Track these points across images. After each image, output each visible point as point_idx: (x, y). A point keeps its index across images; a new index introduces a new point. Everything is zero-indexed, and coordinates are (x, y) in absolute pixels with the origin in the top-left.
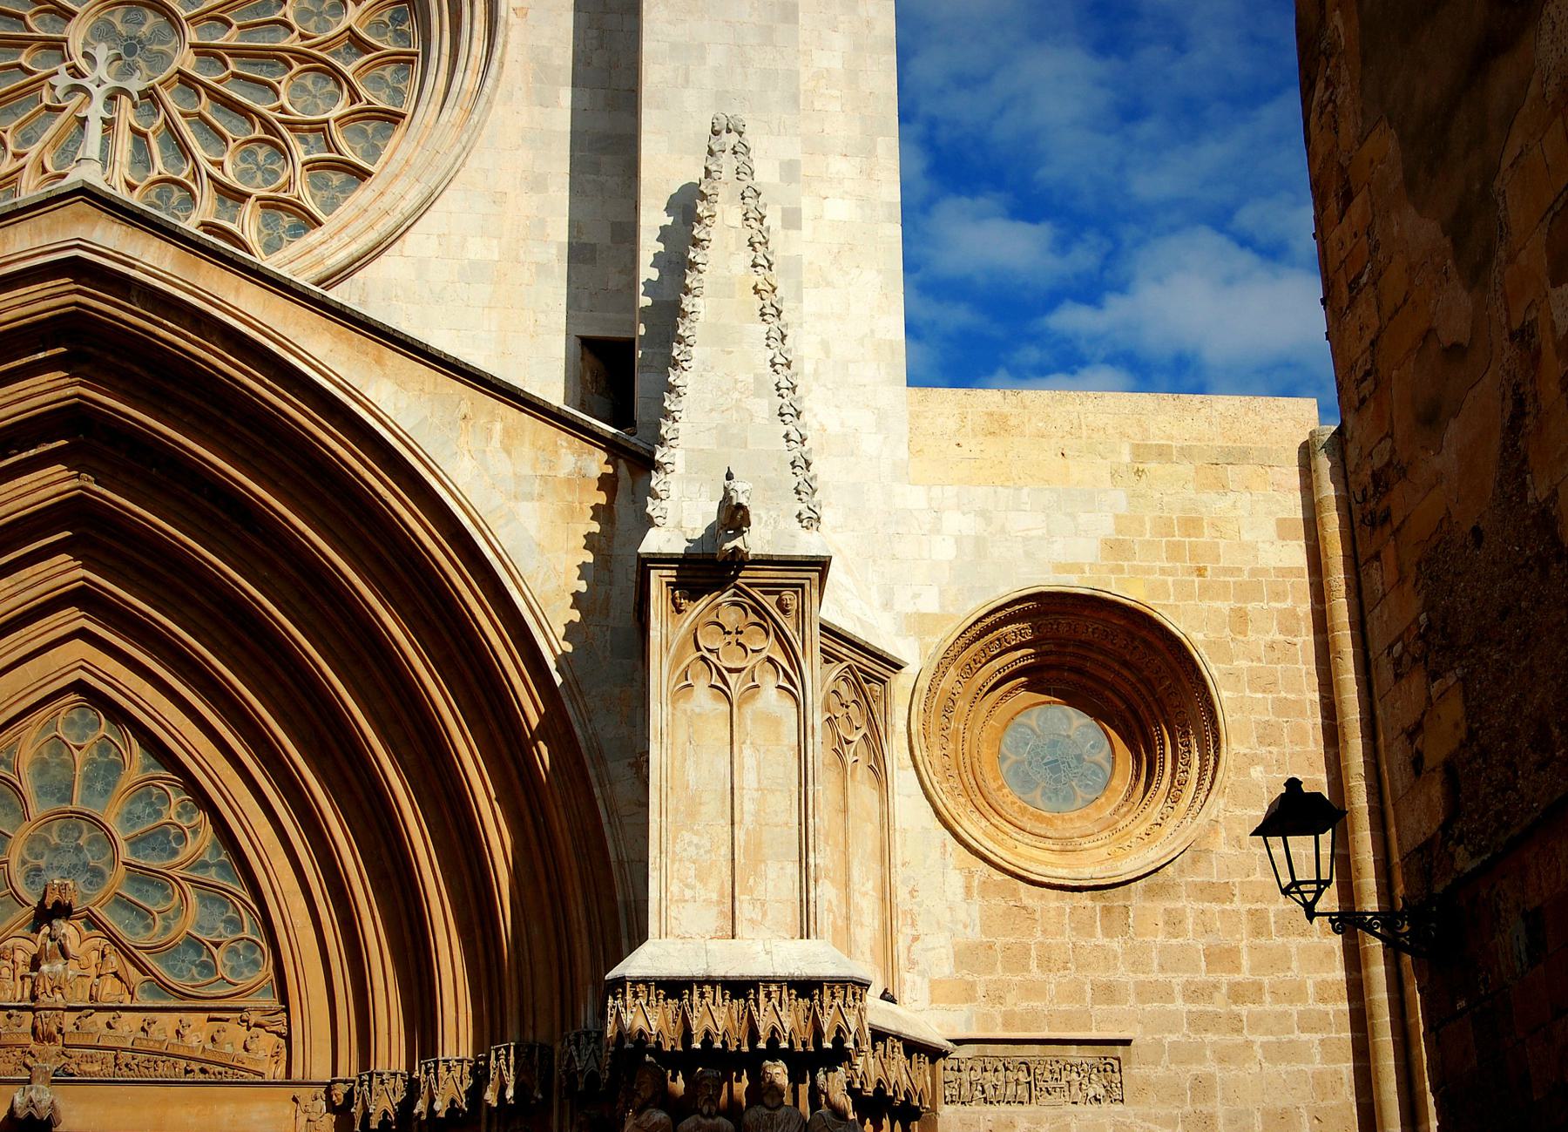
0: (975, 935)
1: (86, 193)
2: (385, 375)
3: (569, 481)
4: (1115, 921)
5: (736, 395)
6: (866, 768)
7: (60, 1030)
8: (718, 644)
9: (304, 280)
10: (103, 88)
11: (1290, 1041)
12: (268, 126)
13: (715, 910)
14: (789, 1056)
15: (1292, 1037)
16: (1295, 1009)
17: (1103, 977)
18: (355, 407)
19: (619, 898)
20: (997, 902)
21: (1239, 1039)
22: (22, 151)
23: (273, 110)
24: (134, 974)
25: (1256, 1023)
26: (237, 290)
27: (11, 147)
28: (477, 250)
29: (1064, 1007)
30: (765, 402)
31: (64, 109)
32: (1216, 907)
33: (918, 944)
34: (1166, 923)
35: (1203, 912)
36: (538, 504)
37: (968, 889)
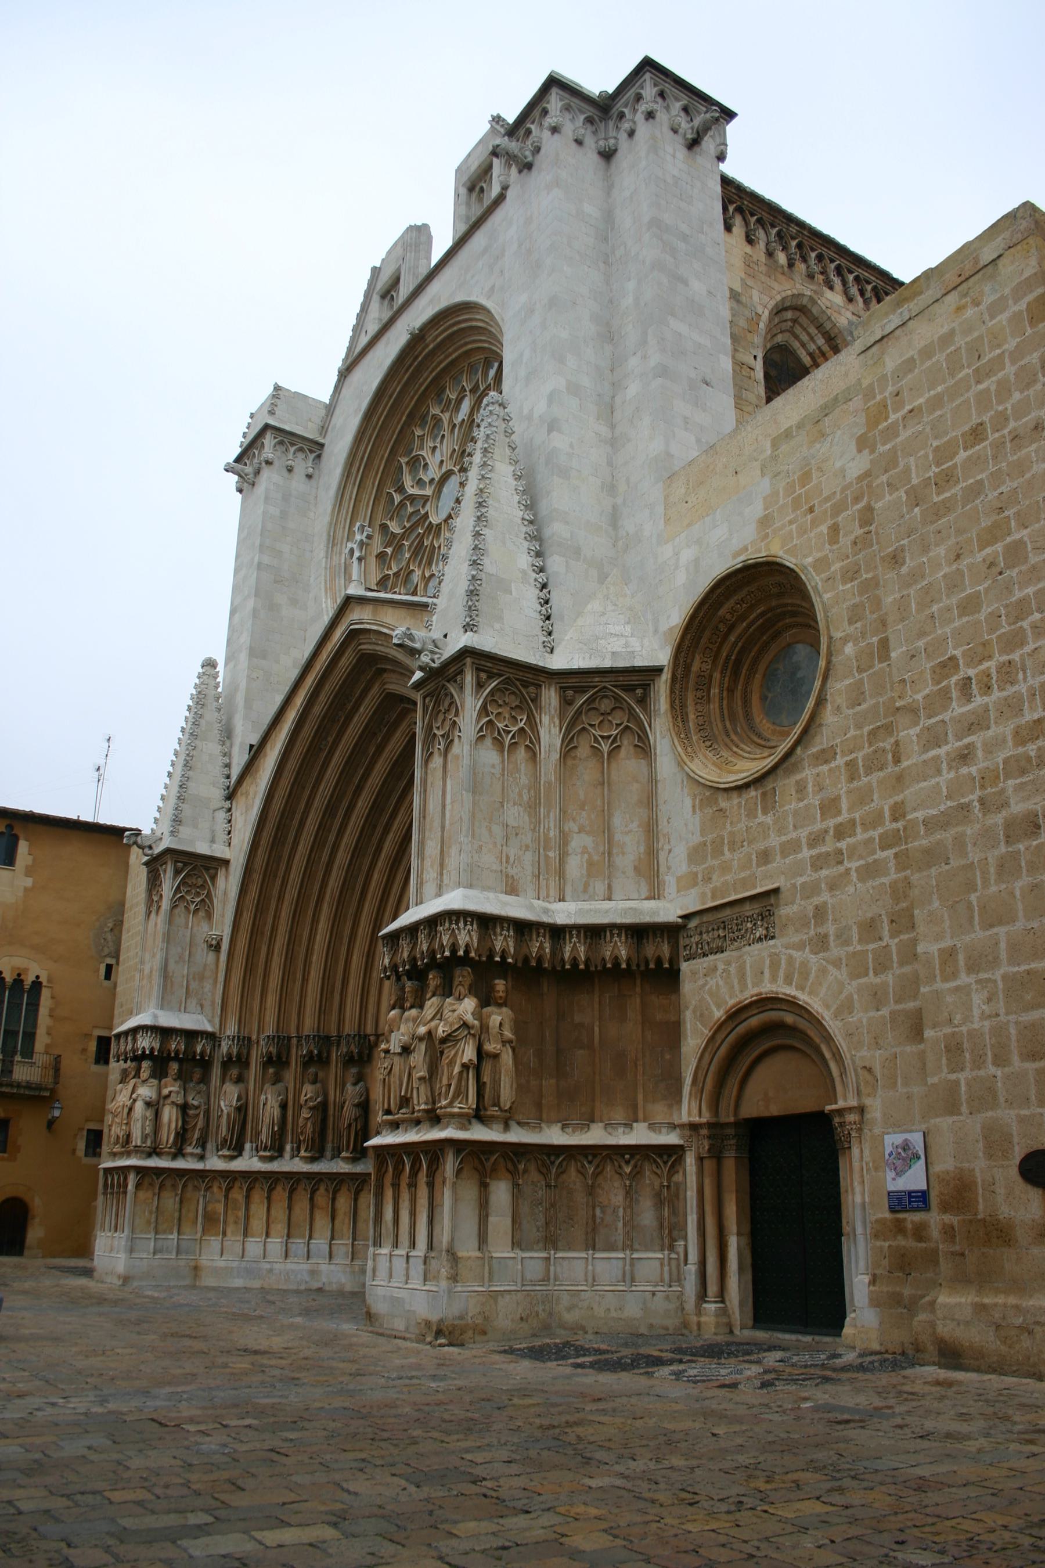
0: (697, 839)
4: (768, 803)
6: (631, 748)
11: (875, 861)
15: (876, 857)
16: (875, 834)
17: (761, 846)
20: (709, 811)
21: (841, 869)
25: (852, 850)
29: (743, 875)
32: (825, 768)
33: (671, 855)
34: (797, 792)
35: (818, 775)
37: (694, 807)
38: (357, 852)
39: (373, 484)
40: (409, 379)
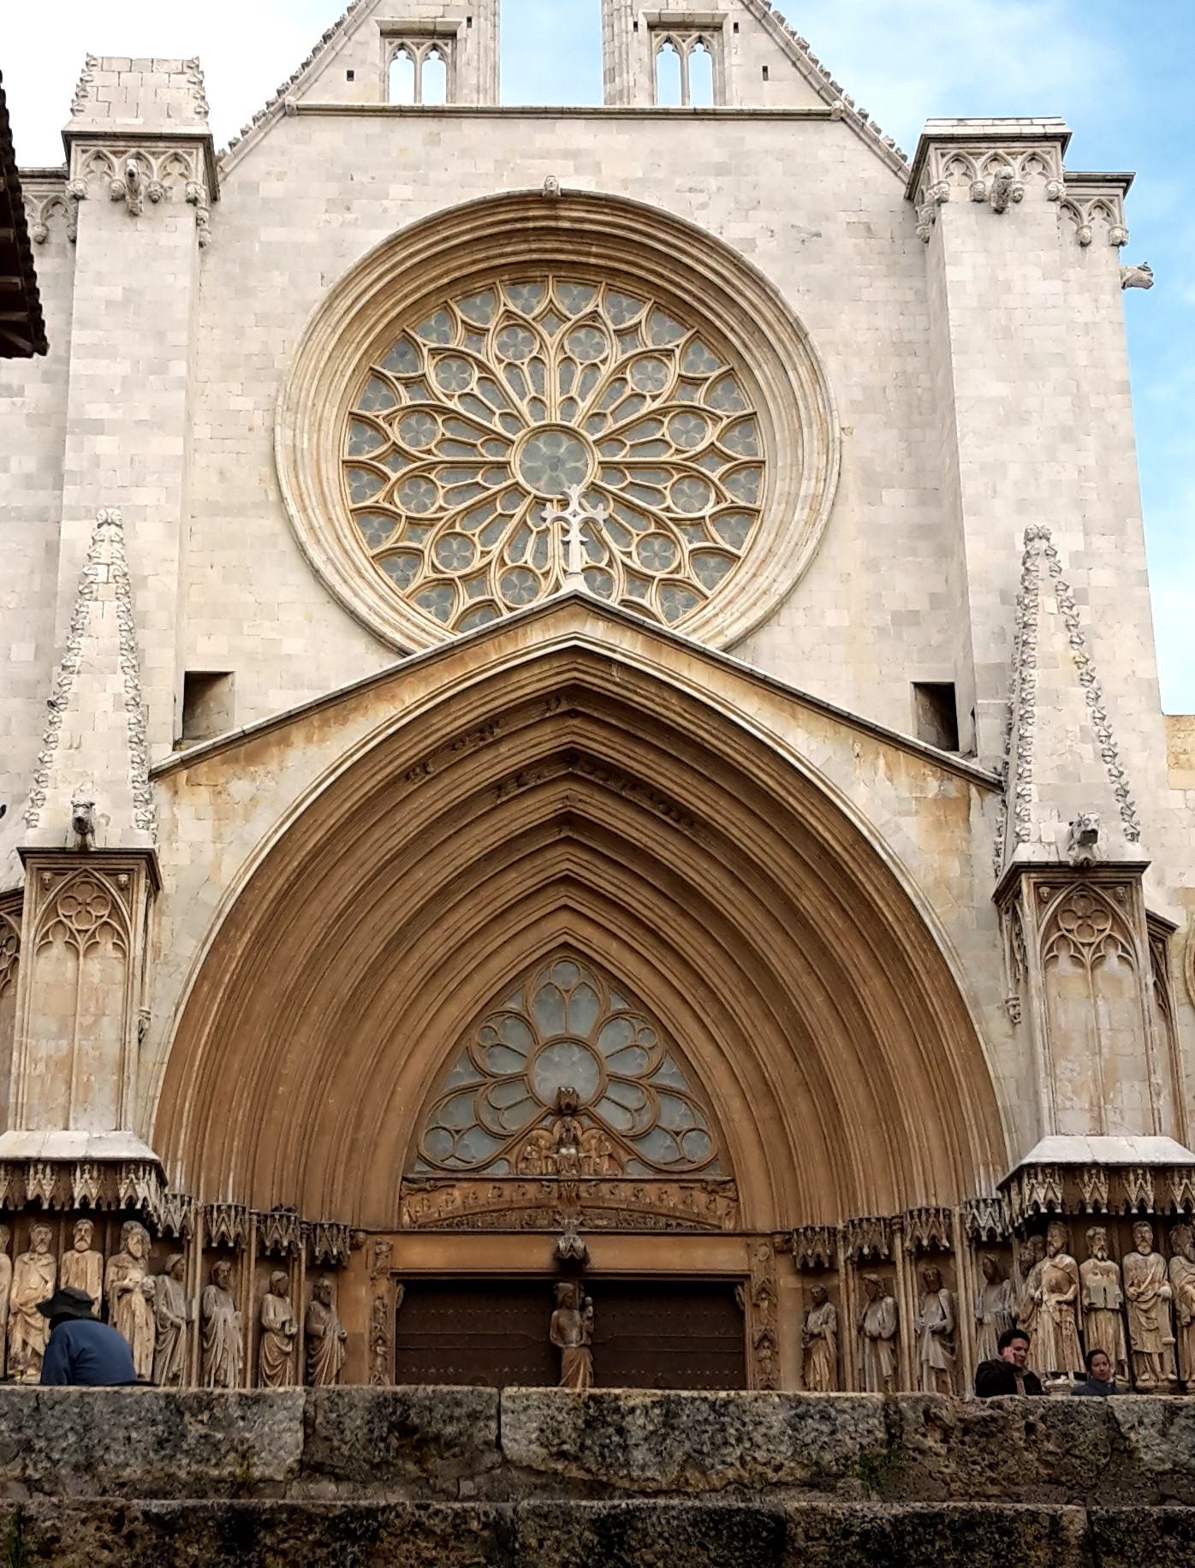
1: (576, 598)
5: (1069, 743)
7: (577, 1195)
8: (1074, 926)
9: (713, 647)
12: (659, 522)
13: (1088, 1115)
14: (1153, 1220)
18: (780, 750)
19: (999, 1103)
22: (486, 549)
23: (662, 510)
24: (624, 1157)
27: (479, 548)
28: (832, 619)
30: (1090, 747)
31: (512, 516)
36: (915, 818)
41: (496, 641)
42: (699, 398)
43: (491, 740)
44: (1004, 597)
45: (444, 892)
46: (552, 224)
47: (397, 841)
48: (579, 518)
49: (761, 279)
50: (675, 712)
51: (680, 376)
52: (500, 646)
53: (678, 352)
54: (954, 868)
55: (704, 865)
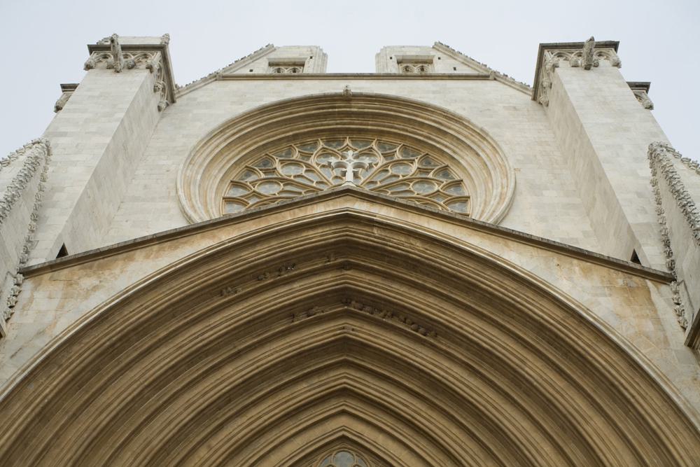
2: (511, 250)
3: (623, 289)
10: (352, 163)
26: (428, 222)
36: (610, 298)
38: (202, 415)
39: (239, 152)
40: (313, 115)
41: (292, 211)
42: (430, 176)
43: (286, 276)
44: (640, 195)
45: (247, 385)
46: (348, 109)
47: (210, 335)
48: (352, 163)
49: (461, 118)
50: (419, 250)
51: (418, 168)
52: (294, 214)
53: (416, 161)
54: (649, 326)
55: (446, 364)
